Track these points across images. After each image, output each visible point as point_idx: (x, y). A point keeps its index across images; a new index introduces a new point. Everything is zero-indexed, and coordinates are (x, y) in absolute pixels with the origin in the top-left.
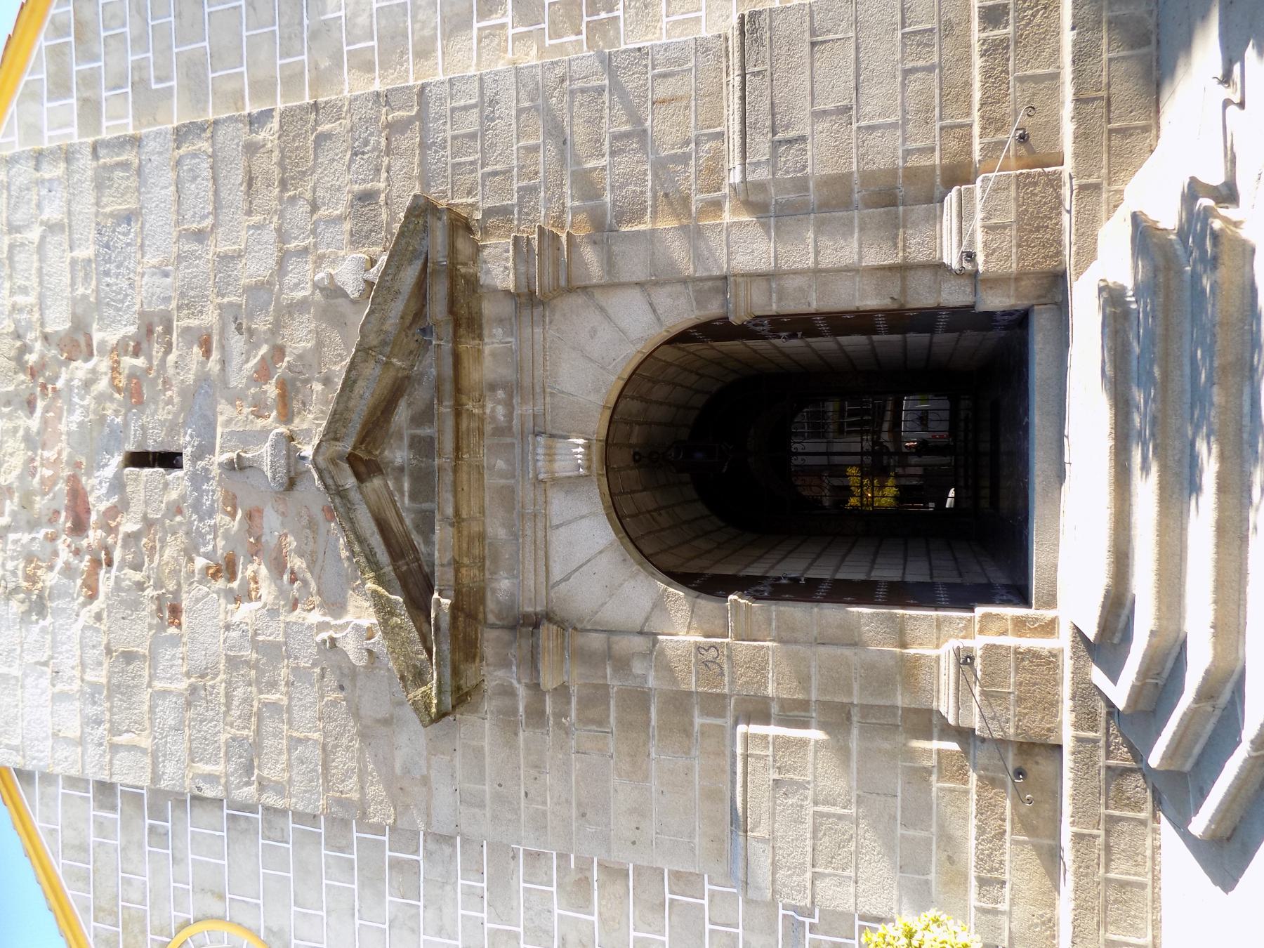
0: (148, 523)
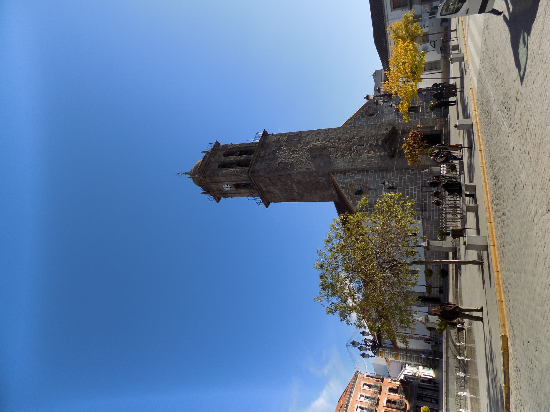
0: (359, 149)
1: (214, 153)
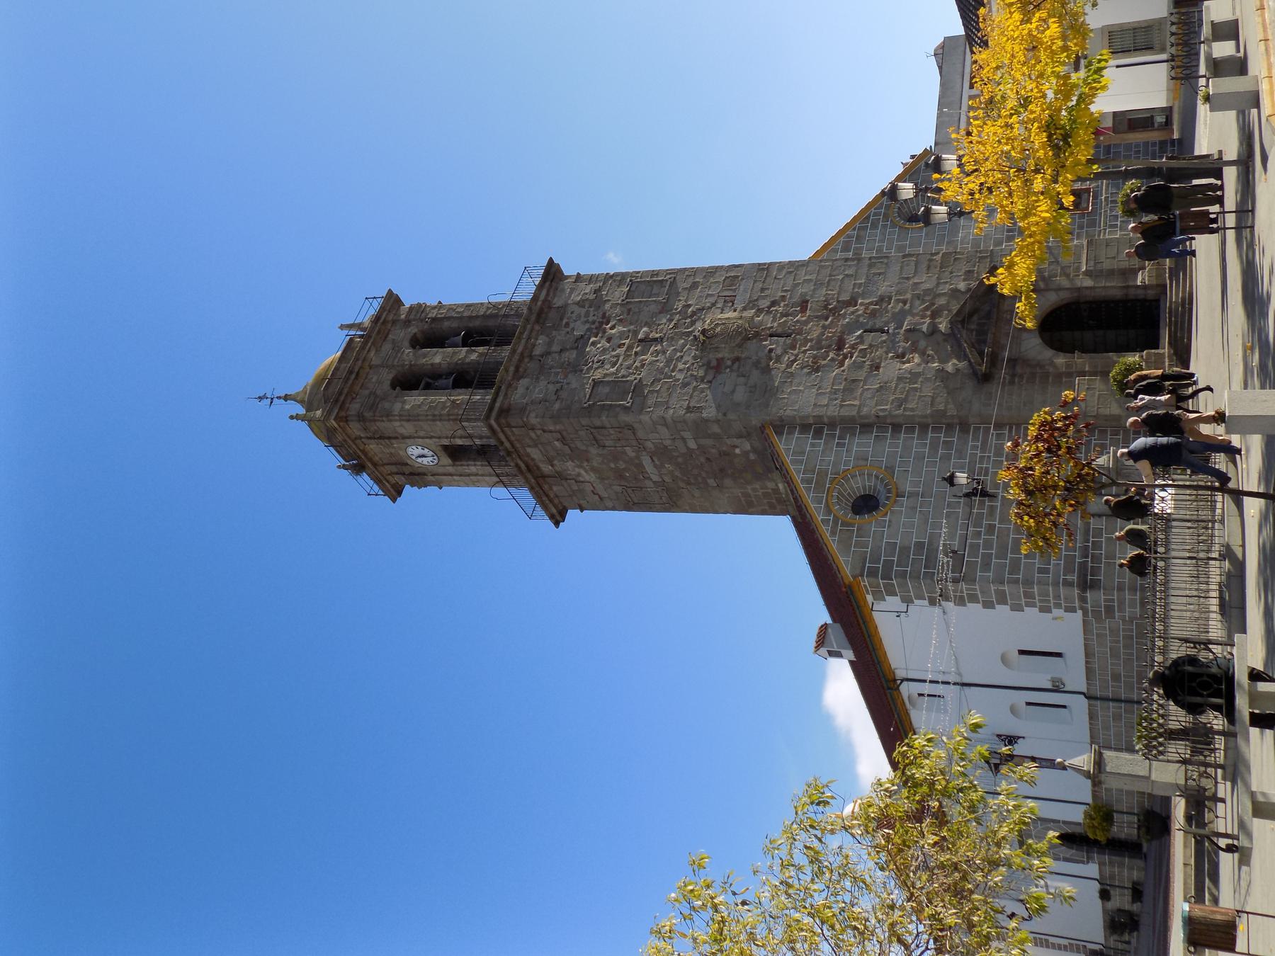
0: (871, 346)
1: (379, 332)
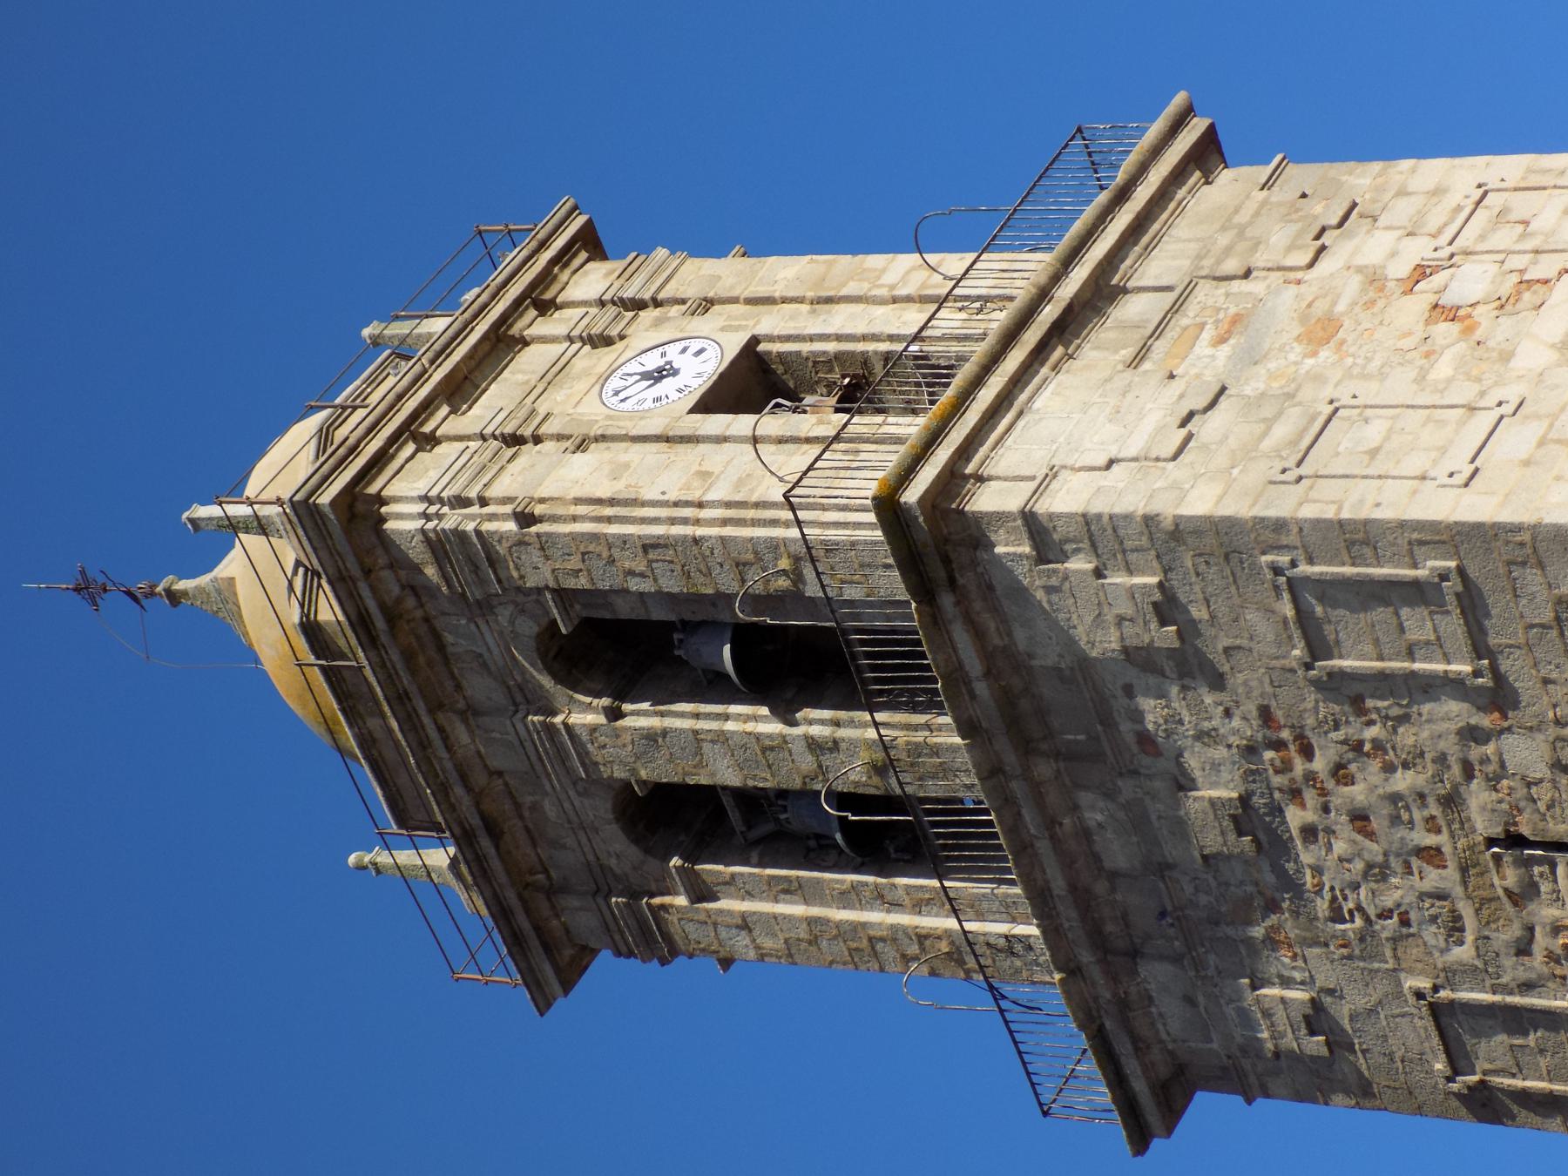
1: (409, 657)
